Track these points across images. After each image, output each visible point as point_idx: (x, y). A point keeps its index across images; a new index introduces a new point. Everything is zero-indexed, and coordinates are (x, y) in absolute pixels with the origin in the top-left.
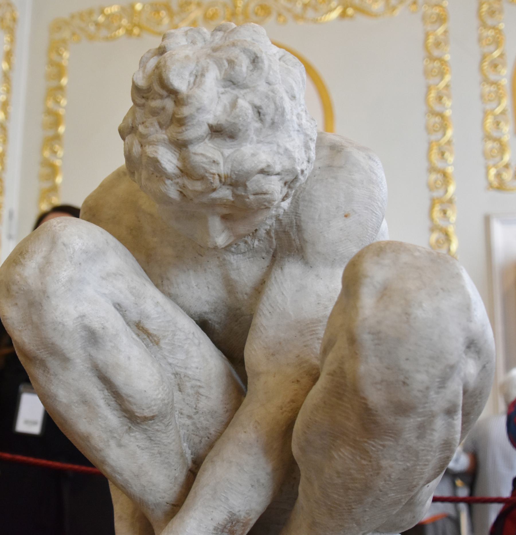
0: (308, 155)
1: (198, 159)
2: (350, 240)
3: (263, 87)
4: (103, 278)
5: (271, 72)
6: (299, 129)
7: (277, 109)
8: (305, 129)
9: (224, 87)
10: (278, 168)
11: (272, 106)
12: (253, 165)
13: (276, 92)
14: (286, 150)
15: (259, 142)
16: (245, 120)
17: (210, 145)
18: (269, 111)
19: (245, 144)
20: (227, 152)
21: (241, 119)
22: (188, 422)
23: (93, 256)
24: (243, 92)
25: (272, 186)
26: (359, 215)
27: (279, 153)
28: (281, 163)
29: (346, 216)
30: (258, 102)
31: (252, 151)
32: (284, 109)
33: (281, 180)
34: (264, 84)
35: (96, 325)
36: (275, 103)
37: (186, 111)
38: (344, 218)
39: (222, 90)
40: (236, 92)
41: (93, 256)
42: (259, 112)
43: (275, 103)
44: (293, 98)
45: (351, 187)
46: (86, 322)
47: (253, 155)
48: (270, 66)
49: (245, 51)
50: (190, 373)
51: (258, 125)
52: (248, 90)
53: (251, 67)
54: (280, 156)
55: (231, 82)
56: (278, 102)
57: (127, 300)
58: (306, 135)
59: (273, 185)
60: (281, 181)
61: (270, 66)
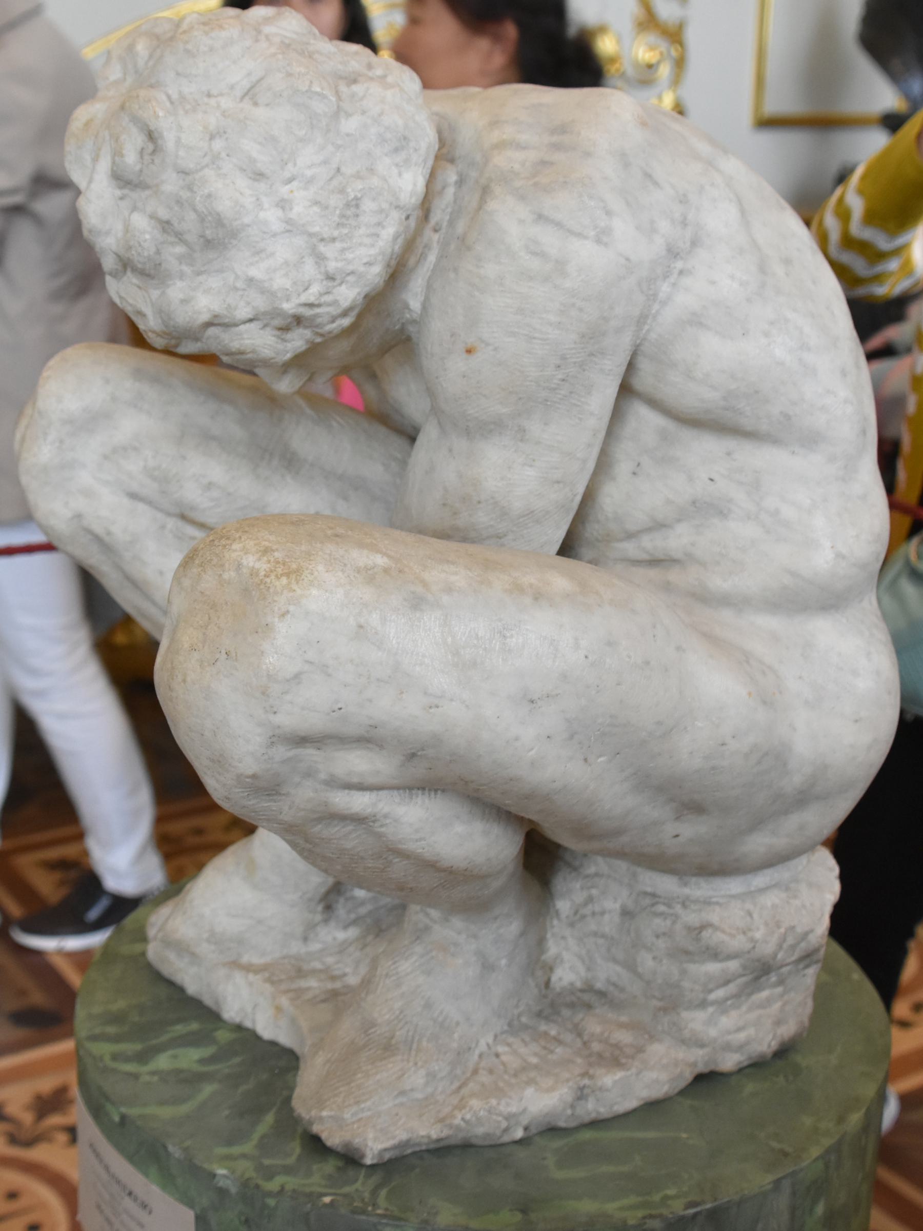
0: (323, 270)
2: (484, 396)
3: (171, 184)
4: (106, 457)
5: (182, 153)
6: (289, 228)
7: (202, 220)
8: (303, 225)
9: (121, 188)
10: (243, 312)
11: (192, 216)
12: (187, 319)
13: (195, 189)
14: (251, 281)
15: (199, 273)
16: (139, 254)
17: (135, 281)
18: (189, 223)
19: (170, 282)
20: (155, 294)
21: (133, 252)
23: (90, 422)
25: (247, 342)
26: (496, 349)
27: (236, 289)
28: (248, 303)
29: (469, 351)
30: (163, 213)
31: (181, 296)
32: (218, 214)
33: (265, 326)
34: (174, 175)
35: (98, 529)
36: (195, 210)
38: (465, 355)
39: (118, 193)
40: (135, 195)
41: (90, 422)
43: (195, 210)
44: (258, 177)
45: (477, 293)
47: (184, 301)
48: (178, 141)
51: (179, 249)
52: (148, 192)
54: (241, 293)
55: (123, 180)
56: (200, 207)
59: (248, 339)
60: (268, 329)
61: (178, 141)
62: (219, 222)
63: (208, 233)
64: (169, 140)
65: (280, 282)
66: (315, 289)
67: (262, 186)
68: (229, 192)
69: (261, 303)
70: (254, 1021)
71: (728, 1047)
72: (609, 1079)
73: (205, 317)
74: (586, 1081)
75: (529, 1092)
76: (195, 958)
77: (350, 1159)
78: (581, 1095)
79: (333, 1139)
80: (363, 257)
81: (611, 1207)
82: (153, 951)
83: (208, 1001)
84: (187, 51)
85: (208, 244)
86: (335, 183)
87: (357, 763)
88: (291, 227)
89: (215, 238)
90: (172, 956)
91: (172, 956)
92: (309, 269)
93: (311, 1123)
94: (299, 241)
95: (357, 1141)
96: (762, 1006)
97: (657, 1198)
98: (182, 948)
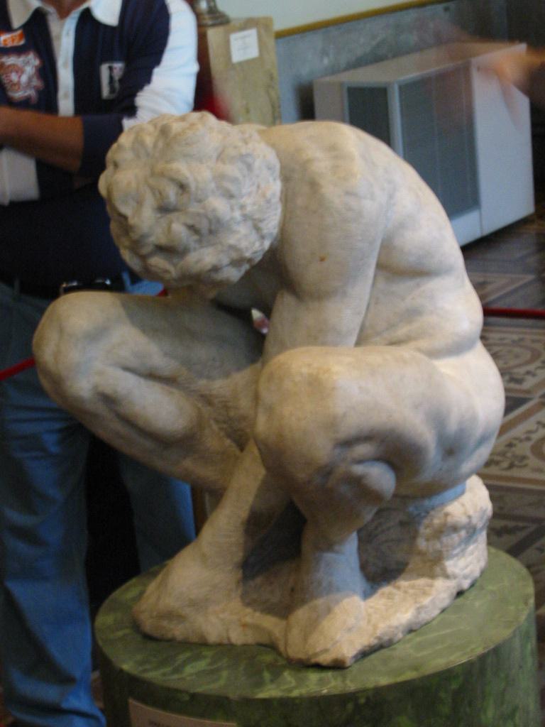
1: (153, 269)
3: (194, 208)
15: (202, 247)
18: (204, 225)
22: (225, 426)
23: (95, 335)
24: (176, 214)
30: (190, 222)
35: (108, 391)
37: (134, 236)
39: (159, 215)
41: (95, 335)
42: (193, 229)
46: (100, 389)
49: (172, 180)
50: (214, 392)
51: (196, 237)
53: (180, 191)
57: (134, 363)
58: (254, 220)
62: (218, 221)
63: (213, 227)
64: (193, 186)
65: (243, 244)
66: (257, 244)
67: (233, 201)
68: (219, 205)
69: (234, 255)
70: (229, 639)
71: (465, 577)
72: (426, 601)
73: (209, 267)
74: (418, 605)
75: (398, 615)
76: (180, 618)
77: (338, 666)
78: (419, 610)
79: (325, 659)
80: (272, 224)
81: (452, 658)
82: (148, 625)
83: (194, 639)
84: (187, 144)
85: (211, 232)
86: (260, 191)
87: (363, 450)
88: (246, 217)
89: (209, 230)
90: (165, 623)
91: (165, 623)
92: (254, 236)
93: (309, 659)
94: (250, 223)
95: (339, 656)
96: (472, 553)
97: (468, 650)
98: (171, 615)
